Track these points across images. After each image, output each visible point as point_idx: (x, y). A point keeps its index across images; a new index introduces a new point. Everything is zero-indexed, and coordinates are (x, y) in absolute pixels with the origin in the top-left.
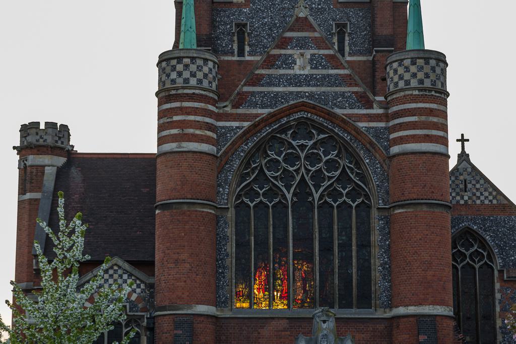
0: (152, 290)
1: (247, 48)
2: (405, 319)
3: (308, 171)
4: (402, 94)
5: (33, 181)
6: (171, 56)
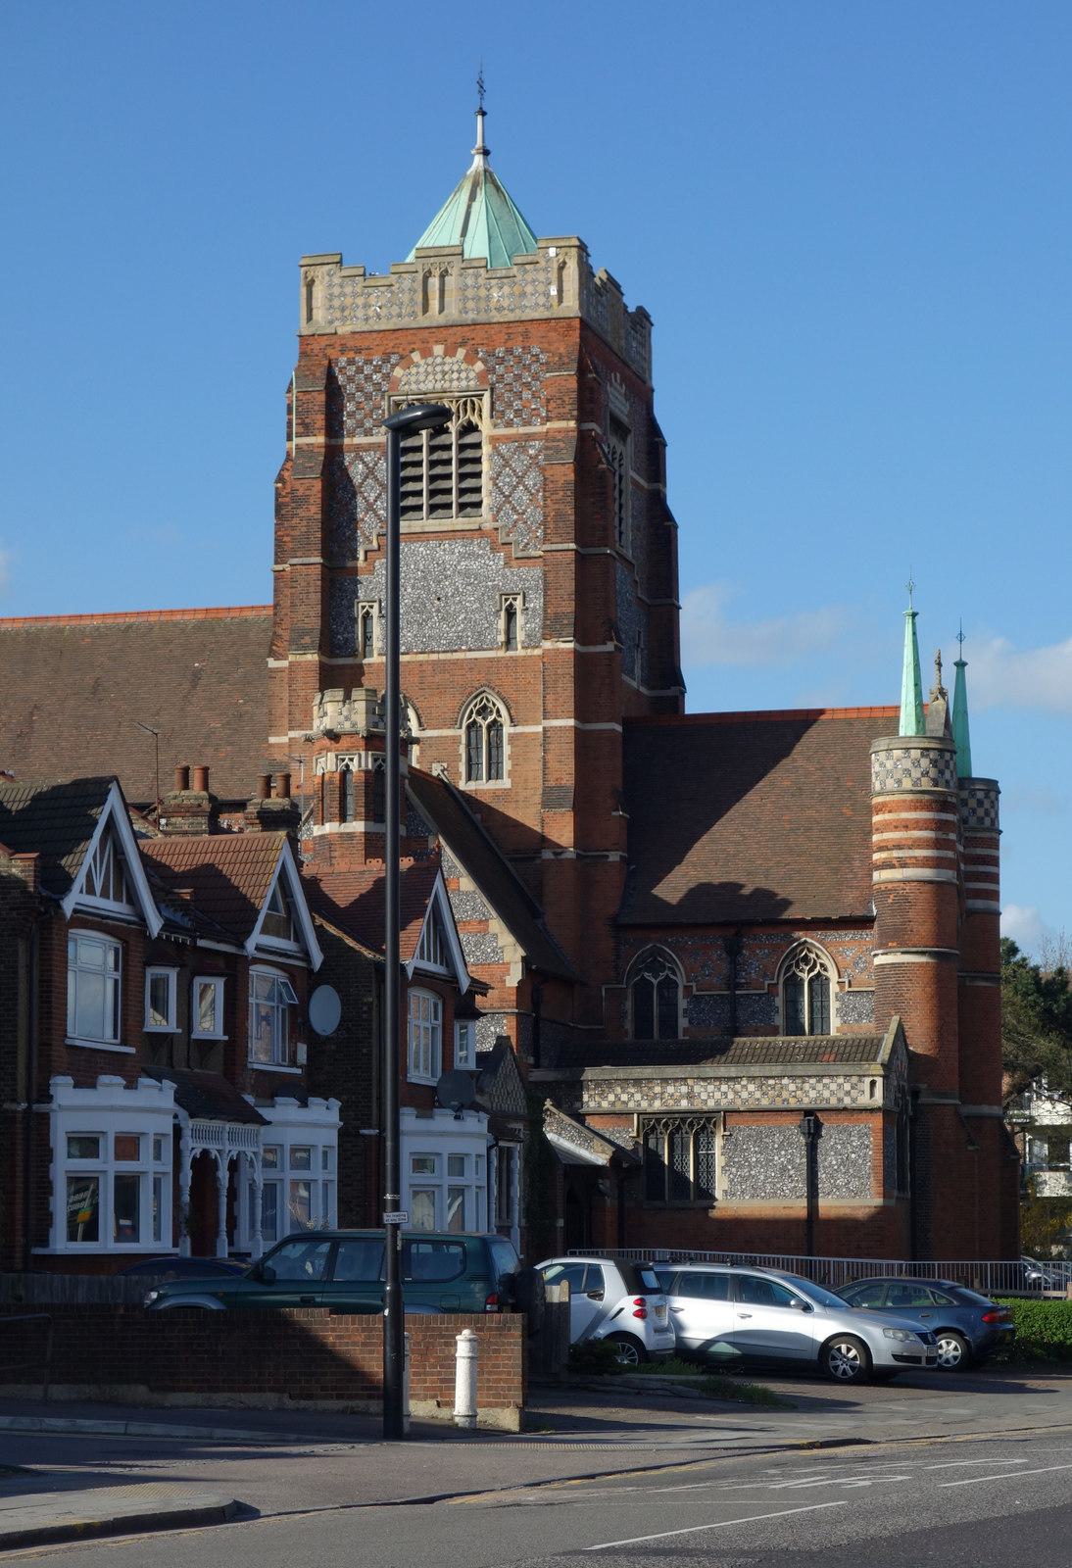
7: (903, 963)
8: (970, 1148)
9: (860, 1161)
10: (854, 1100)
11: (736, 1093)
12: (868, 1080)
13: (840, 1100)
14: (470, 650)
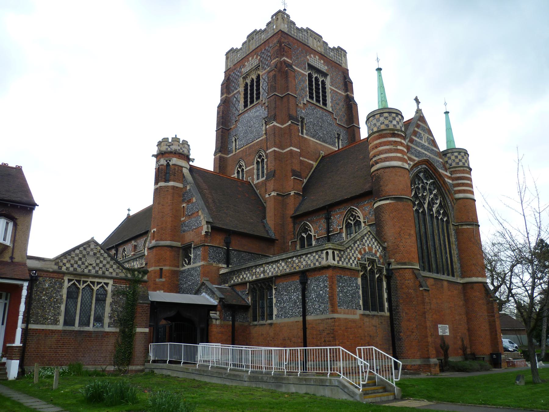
0: (385, 252)
1: (305, 131)
2: (477, 284)
3: (430, 197)
4: (462, 169)
5: (176, 175)
7: (380, 205)
8: (421, 289)
9: (324, 294)
10: (320, 263)
11: (278, 267)
12: (325, 252)
13: (315, 264)
14: (256, 139)
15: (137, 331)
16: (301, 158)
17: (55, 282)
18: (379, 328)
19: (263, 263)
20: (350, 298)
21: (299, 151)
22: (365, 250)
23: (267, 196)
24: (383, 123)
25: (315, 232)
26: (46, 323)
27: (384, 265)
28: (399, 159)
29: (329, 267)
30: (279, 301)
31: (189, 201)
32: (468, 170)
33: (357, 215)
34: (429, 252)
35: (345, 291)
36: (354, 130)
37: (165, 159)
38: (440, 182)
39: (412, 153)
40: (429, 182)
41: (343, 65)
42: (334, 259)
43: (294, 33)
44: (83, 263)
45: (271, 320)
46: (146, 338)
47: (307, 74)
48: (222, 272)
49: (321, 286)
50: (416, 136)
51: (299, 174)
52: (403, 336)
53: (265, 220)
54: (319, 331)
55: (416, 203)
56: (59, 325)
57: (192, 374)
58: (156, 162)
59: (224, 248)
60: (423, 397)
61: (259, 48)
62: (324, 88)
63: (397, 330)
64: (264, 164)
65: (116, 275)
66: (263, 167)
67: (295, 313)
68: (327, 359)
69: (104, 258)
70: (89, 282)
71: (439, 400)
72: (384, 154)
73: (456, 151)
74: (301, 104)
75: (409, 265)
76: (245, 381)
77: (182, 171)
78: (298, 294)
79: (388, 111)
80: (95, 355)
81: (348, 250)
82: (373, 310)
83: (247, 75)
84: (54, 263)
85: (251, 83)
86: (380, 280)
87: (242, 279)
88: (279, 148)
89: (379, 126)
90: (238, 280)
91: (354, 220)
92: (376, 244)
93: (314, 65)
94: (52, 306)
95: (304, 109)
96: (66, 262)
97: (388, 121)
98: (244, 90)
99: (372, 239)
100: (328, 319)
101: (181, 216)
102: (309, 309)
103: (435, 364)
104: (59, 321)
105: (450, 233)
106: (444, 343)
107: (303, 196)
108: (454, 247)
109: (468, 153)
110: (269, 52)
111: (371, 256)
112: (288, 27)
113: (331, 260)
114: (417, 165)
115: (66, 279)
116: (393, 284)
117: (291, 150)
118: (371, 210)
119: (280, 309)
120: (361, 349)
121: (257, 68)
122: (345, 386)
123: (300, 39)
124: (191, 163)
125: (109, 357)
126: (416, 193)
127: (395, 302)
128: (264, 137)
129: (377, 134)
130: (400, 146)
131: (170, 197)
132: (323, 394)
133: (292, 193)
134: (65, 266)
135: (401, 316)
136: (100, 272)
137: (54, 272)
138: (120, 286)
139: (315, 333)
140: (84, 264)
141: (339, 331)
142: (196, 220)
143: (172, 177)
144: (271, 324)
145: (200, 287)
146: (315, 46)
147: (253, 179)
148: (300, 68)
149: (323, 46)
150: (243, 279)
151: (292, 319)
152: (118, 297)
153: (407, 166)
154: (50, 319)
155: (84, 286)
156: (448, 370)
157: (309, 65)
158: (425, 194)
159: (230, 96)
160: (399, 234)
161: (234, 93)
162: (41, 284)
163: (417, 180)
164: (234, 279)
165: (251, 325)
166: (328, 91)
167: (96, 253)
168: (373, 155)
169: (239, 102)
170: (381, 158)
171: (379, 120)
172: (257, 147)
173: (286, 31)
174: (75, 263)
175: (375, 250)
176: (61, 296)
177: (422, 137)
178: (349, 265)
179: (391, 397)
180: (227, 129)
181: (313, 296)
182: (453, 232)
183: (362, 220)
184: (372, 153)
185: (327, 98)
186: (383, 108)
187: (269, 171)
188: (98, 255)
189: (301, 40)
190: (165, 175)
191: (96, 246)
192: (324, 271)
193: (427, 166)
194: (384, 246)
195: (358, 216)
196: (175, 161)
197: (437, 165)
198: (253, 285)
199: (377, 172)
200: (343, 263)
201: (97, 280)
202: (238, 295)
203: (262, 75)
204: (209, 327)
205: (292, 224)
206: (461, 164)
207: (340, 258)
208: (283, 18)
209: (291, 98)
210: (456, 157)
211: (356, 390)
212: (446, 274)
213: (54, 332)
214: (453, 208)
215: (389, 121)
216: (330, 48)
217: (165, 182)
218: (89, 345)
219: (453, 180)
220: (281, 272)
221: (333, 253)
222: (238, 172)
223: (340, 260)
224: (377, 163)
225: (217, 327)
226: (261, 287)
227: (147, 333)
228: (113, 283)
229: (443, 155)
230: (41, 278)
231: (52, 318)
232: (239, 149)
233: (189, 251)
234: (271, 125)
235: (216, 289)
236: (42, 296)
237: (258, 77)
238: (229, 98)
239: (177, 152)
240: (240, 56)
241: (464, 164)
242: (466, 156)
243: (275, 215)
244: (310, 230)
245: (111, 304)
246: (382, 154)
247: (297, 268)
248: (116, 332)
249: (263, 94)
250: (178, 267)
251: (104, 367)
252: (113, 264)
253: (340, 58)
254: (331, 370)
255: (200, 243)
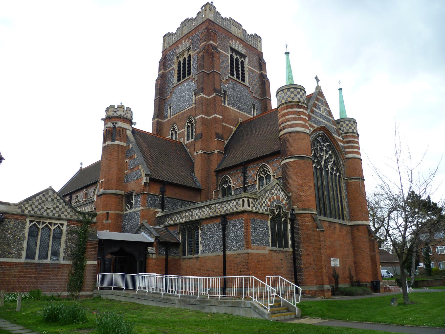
0: (290, 200)
1: (227, 102)
2: (362, 226)
4: (351, 134)
5: (121, 135)
6: (284, 89)
7: (286, 163)
8: (318, 230)
9: (240, 234)
10: (237, 209)
11: (204, 212)
12: (241, 200)
13: (233, 209)
14: (188, 108)
15: (87, 263)
16: (224, 124)
17: (18, 223)
18: (284, 261)
19: (191, 208)
20: (261, 237)
21: (222, 117)
22: (273, 198)
23: (195, 154)
24: (290, 96)
25: (233, 183)
26: (11, 257)
27: (289, 210)
28: (303, 126)
29: (244, 212)
30: (204, 239)
31: (131, 157)
32: (356, 135)
33: (267, 170)
34: (325, 200)
35: (257, 231)
36: (266, 102)
37: (112, 122)
38: (334, 145)
39: (313, 121)
40: (325, 145)
41: (259, 49)
42: (249, 206)
43: (219, 21)
44: (42, 208)
45: (197, 254)
46: (95, 269)
47: (229, 56)
48: (158, 215)
49: (238, 227)
50: (315, 108)
51: (221, 136)
52: (303, 267)
53: (193, 174)
54: (236, 263)
55: (315, 161)
56: (22, 258)
57: (132, 298)
58: (105, 125)
59: (159, 196)
60: (318, 316)
61: (190, 33)
62: (243, 67)
63: (298, 262)
64: (193, 127)
65: (70, 217)
66: (192, 131)
67: (217, 249)
68: (242, 286)
69: (60, 204)
70: (47, 223)
71: (330, 318)
72: (290, 121)
73: (347, 120)
74: (224, 80)
75: (308, 211)
76: (176, 304)
77: (126, 132)
78: (219, 234)
79: (293, 87)
80: (52, 283)
81: (260, 199)
82: (279, 247)
83: (180, 54)
84: (17, 207)
85: (183, 61)
86: (285, 223)
87: (174, 222)
88: (206, 115)
89: (287, 99)
90: (171, 222)
91: (265, 174)
92: (282, 193)
93: (235, 48)
94: (16, 243)
95: (226, 84)
96: (28, 206)
97: (294, 95)
98: (178, 67)
99: (279, 190)
100: (244, 253)
101: (124, 169)
102: (228, 246)
103: (328, 290)
104: (22, 255)
105: (341, 185)
106: (335, 273)
107: (225, 154)
108: (344, 196)
109: (357, 122)
110: (198, 36)
111: (279, 203)
112: (214, 17)
113: (246, 206)
114: (317, 130)
115: (28, 220)
116: (295, 226)
117: (215, 116)
118: (279, 166)
119: (205, 246)
120: (269, 277)
121: (189, 49)
122: (256, 307)
123: (224, 26)
124: (133, 126)
125: (64, 284)
126: (315, 153)
127: (297, 240)
128: (194, 106)
129: (285, 105)
130: (303, 115)
131: (115, 154)
132: (238, 314)
133: (216, 152)
134: (27, 209)
135: (302, 251)
136: (57, 215)
137: (18, 215)
138: (73, 226)
139: (233, 265)
140: (43, 208)
141: (252, 264)
142: (137, 173)
143: (118, 137)
144: (197, 258)
145: (140, 228)
146: (236, 33)
147: (184, 140)
148: (224, 50)
149: (243, 33)
150: (175, 221)
151: (215, 254)
152: (71, 236)
153: (308, 132)
154: (14, 253)
155: (43, 227)
156: (338, 295)
157: (231, 48)
158: (322, 154)
159: (166, 71)
160: (301, 186)
161: (170, 69)
162: (6, 224)
163: (316, 143)
164: (168, 221)
165: (181, 258)
166: (246, 70)
167: (53, 199)
168: (281, 122)
169: (174, 77)
170: (288, 125)
171: (287, 94)
172: (188, 114)
173: (213, 19)
174: (35, 208)
175: (282, 198)
176: (24, 234)
177: (321, 109)
178: (261, 211)
179: (293, 316)
180: (164, 99)
181: (231, 235)
182: (343, 185)
183: (271, 174)
184: (280, 121)
185: (245, 76)
186: (290, 84)
187: (197, 134)
188: (55, 201)
189: (225, 28)
190: (112, 136)
191: (53, 193)
192: (240, 215)
193: (324, 132)
194: (289, 195)
195: (269, 171)
196: (120, 124)
197: (332, 131)
198: (183, 226)
199: (284, 136)
200: (256, 209)
201: (54, 221)
202: (171, 234)
203: (193, 55)
204: (147, 260)
205: (215, 177)
206: (351, 130)
207: (254, 205)
208: (210, 9)
209: (216, 75)
210: (347, 125)
211: (265, 311)
212: (337, 218)
213: (18, 265)
214: (344, 166)
215: (295, 95)
216: (248, 35)
217: (112, 141)
218: (46, 275)
219: (344, 144)
220: (206, 216)
221: (248, 201)
222: (172, 134)
223: (254, 206)
224: (284, 128)
225: (153, 260)
226: (190, 227)
227: (95, 265)
228: (68, 224)
229: (337, 123)
230: (7, 219)
231: (16, 253)
232: (173, 115)
233: (131, 198)
234: (199, 96)
235: (153, 229)
236: (7, 235)
237: (190, 57)
238: (166, 73)
239: (122, 117)
240: (175, 39)
241: (353, 130)
242: (354, 124)
243: (202, 169)
244: (230, 182)
245: (65, 241)
246: (288, 121)
247: (219, 212)
248: (70, 264)
249: (193, 71)
250: (122, 211)
251: (59, 293)
252: (67, 208)
253: (256, 43)
254: (245, 295)
255: (140, 191)
